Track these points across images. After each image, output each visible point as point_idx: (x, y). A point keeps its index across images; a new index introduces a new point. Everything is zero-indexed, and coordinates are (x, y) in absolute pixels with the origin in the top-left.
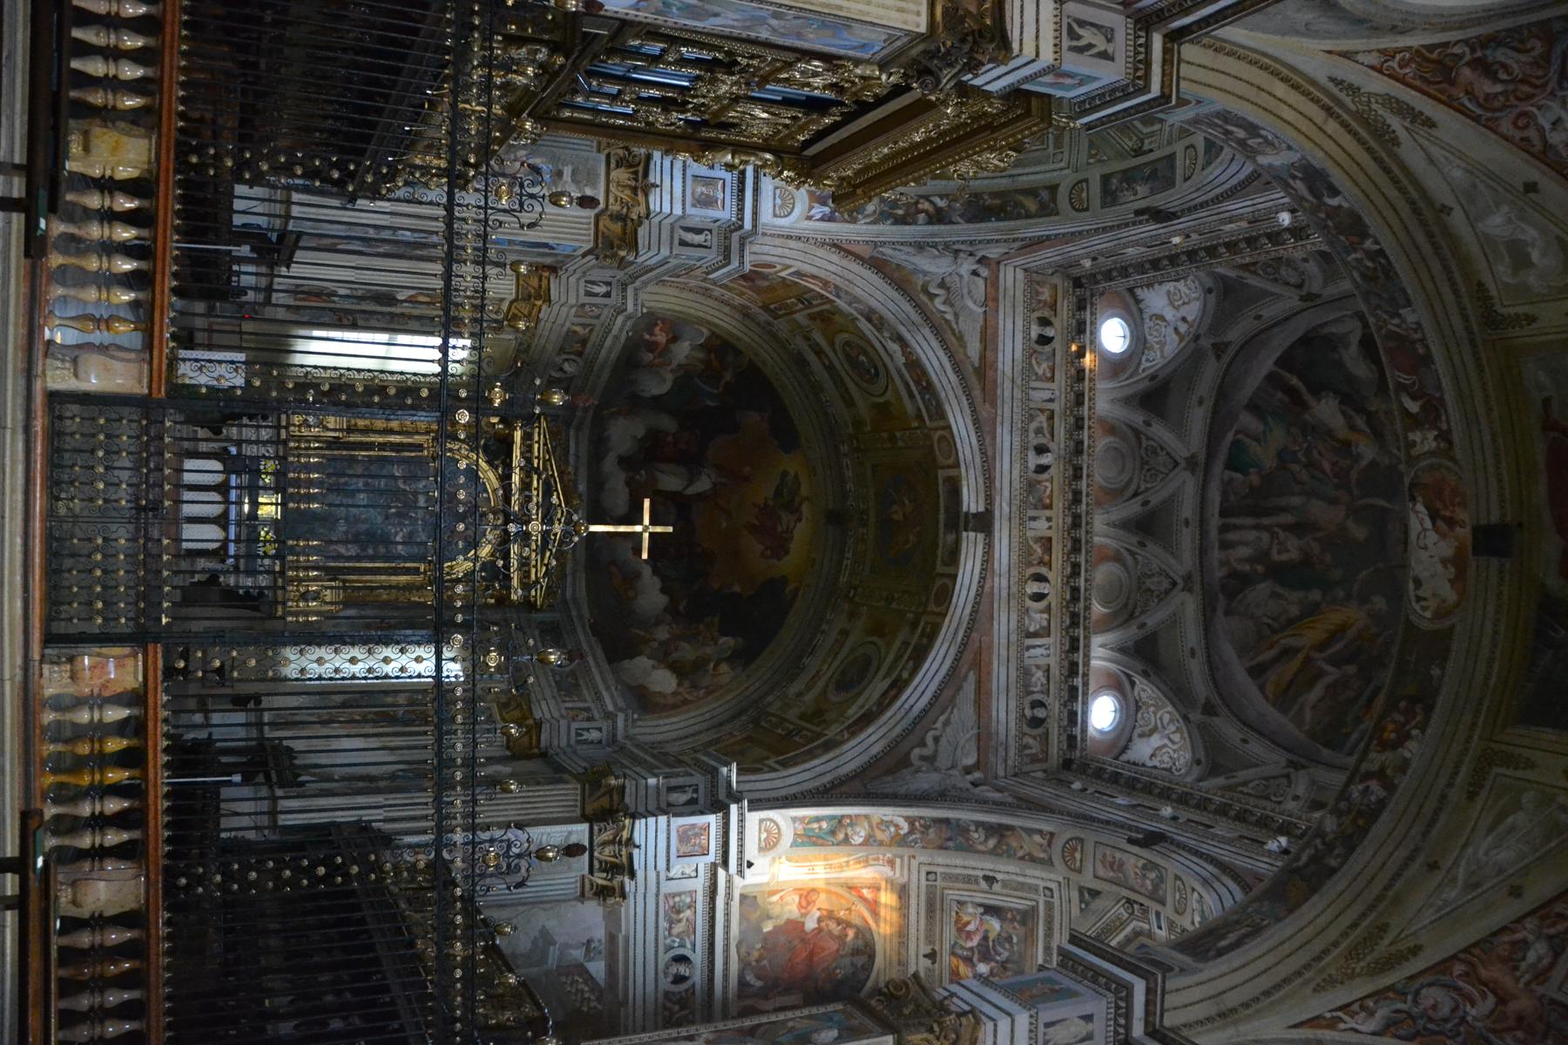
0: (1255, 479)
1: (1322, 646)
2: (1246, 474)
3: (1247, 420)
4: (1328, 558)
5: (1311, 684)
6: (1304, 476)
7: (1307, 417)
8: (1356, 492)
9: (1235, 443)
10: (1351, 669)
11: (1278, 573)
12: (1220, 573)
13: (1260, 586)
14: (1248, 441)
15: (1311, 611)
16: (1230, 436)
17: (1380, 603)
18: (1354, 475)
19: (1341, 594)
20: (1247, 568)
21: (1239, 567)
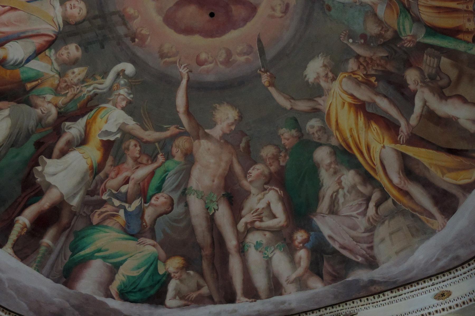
0: (174, 264)
1: (390, 126)
2: (168, 277)
3: (89, 283)
4: (268, 151)
5: (448, 123)
6: (160, 200)
7: (75, 202)
8: (173, 130)
9: (124, 295)
10: (412, 76)
11: (301, 210)
12: (317, 286)
13: (326, 232)
14: (120, 278)
15: (345, 156)
16: (115, 304)
17: (315, 69)
18: (150, 135)
19: (313, 125)
20: (302, 254)
21: (304, 263)
